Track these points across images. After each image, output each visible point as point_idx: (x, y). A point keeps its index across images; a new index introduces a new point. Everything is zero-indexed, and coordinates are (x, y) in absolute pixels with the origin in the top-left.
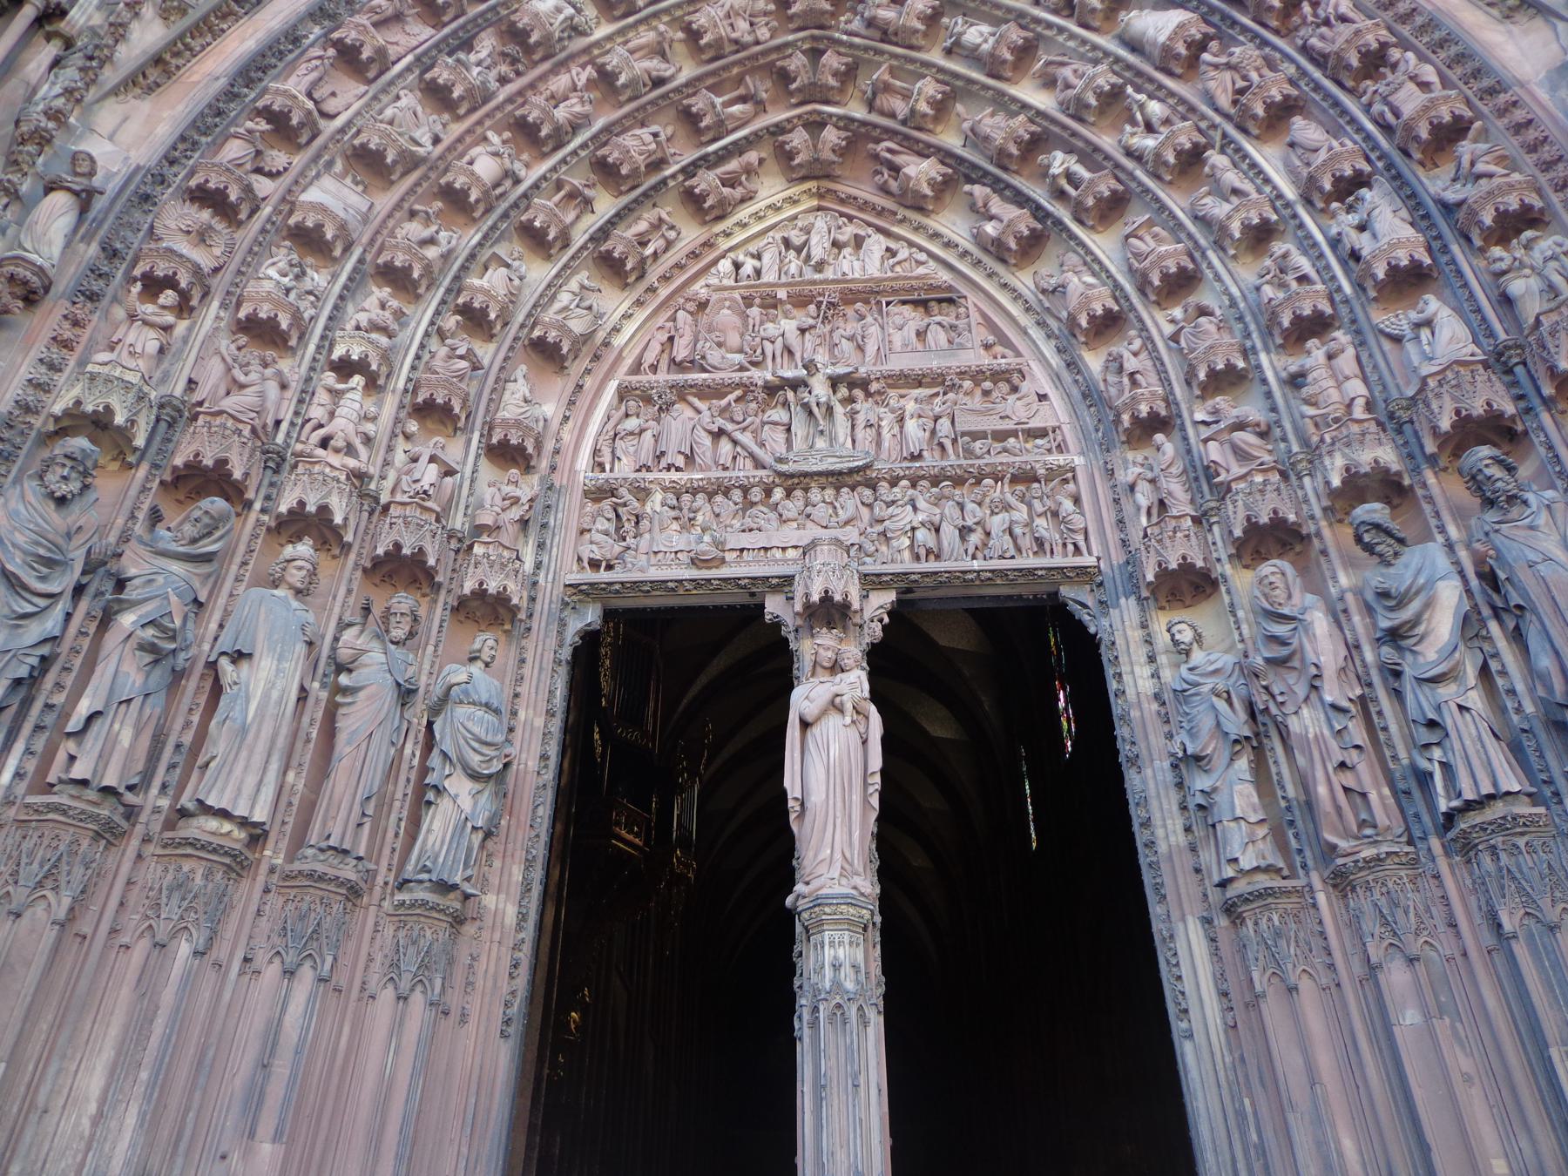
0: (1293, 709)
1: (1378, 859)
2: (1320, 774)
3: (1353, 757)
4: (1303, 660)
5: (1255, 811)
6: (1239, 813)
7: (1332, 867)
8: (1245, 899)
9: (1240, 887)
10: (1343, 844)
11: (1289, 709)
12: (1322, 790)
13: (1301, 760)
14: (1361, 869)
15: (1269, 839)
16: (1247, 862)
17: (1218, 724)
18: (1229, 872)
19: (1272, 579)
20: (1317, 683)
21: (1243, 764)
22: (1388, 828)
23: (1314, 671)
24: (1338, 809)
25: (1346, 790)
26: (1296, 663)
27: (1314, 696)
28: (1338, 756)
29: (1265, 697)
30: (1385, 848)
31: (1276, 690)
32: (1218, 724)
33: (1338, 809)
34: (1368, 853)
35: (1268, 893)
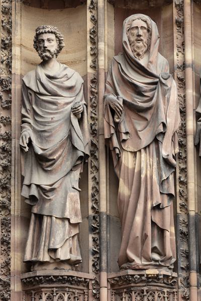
0: (131, 149)
1: (156, 278)
2: (140, 207)
3: (166, 202)
4: (156, 115)
5: (76, 215)
6: (67, 215)
7: (122, 273)
8: (49, 279)
9: (50, 271)
10: (138, 262)
11: (128, 146)
12: (138, 219)
13: (124, 189)
14: (142, 281)
15: (76, 238)
16: (62, 255)
17: (70, 137)
18: (45, 257)
19: (141, 32)
20: (160, 138)
21: (76, 174)
22: (170, 258)
23: (161, 129)
24: (144, 237)
25: (153, 224)
26: (148, 116)
27: (153, 148)
28: (157, 199)
29: (113, 131)
30: (164, 272)
31: (123, 129)
32: (70, 137)
33: (144, 237)
34: (152, 272)
35: (70, 280)
